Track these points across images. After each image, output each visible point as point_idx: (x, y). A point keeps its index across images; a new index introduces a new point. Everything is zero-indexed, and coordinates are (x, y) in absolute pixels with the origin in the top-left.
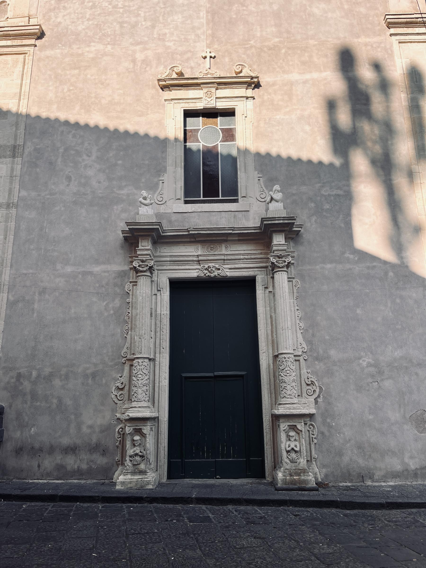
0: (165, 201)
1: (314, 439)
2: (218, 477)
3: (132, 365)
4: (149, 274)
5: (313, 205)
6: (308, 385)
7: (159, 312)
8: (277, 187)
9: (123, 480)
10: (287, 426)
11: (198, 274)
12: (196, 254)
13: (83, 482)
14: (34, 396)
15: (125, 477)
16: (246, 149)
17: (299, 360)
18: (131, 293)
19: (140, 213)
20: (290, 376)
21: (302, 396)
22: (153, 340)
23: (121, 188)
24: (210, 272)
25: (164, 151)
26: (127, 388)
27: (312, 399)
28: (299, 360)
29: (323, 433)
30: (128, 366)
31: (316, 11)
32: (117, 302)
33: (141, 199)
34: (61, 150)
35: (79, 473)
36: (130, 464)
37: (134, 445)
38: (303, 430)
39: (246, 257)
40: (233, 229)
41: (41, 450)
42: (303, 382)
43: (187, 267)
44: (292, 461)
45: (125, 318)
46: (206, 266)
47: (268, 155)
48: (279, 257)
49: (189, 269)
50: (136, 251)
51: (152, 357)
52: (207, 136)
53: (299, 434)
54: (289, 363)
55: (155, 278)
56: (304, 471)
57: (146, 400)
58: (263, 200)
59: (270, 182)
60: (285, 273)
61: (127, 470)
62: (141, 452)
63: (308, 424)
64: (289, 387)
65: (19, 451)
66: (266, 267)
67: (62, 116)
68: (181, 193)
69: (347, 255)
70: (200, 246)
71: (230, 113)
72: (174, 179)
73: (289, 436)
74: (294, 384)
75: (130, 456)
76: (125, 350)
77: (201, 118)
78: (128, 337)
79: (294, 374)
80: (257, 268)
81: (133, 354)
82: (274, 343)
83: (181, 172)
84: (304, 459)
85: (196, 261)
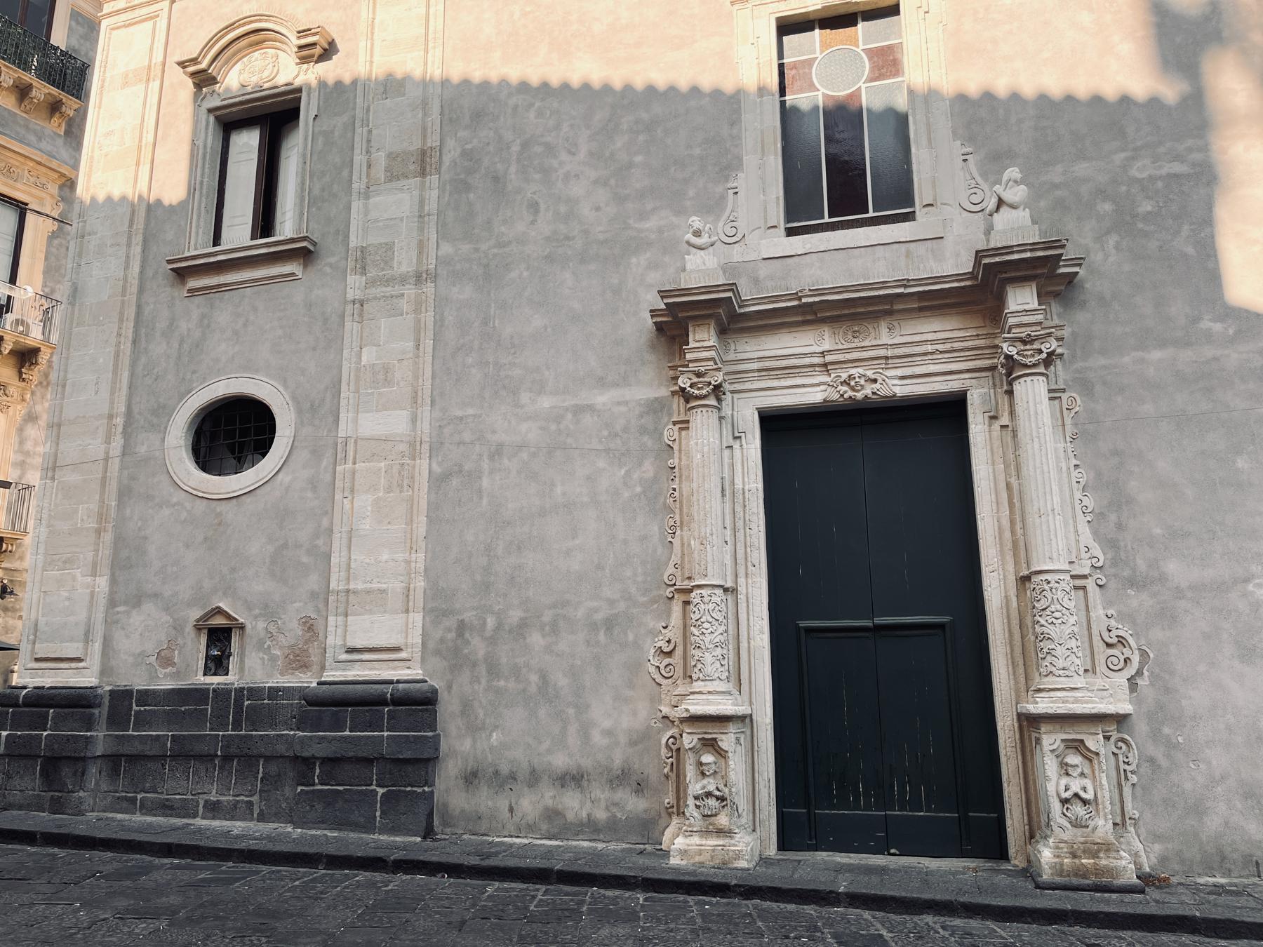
1: (1129, 775)
2: (893, 851)
3: (687, 603)
4: (713, 402)
5: (1107, 207)
6: (1109, 645)
7: (739, 484)
8: (1013, 172)
9: (685, 847)
10: (1058, 742)
11: (826, 394)
12: (821, 349)
13: (600, 846)
14: (493, 670)
15: (688, 841)
16: (930, 90)
17: (1084, 588)
18: (676, 447)
19: (689, 266)
20: (1063, 625)
21: (1094, 672)
22: (729, 548)
23: (643, 216)
24: (853, 389)
25: (735, 122)
26: (679, 652)
27: (1121, 679)
28: (1084, 588)
29: (1152, 760)
30: (680, 604)
32: (649, 469)
33: (689, 237)
34: (515, 148)
35: (590, 828)
36: (695, 814)
37: (703, 774)
38: (1102, 751)
39: (940, 347)
40: (906, 283)
41: (513, 777)
42: (1096, 639)
43: (799, 381)
44: (1076, 824)
45: (667, 502)
46: (844, 376)
47: (988, 96)
48: (1024, 342)
49: (804, 386)
50: (682, 354)
51: (729, 584)
52: (834, 71)
53: (1091, 761)
54: (1060, 594)
55: (726, 411)
57: (724, 677)
58: (977, 208)
59: (995, 162)
60: (1041, 378)
61: (690, 825)
62: (718, 789)
63: (1113, 739)
64: (1060, 651)
65: (471, 778)
66: (992, 368)
67: (514, 73)
68: (777, 212)
69: (1206, 324)
70: (826, 331)
72: (761, 182)
73: (1067, 764)
74: (1073, 643)
75: (696, 798)
76: (671, 570)
77: (817, 31)
78: (677, 542)
79: (1072, 620)
80: (968, 371)
81: (689, 578)
82: (1019, 547)
83: (775, 164)
84: (1106, 820)
85: (819, 365)
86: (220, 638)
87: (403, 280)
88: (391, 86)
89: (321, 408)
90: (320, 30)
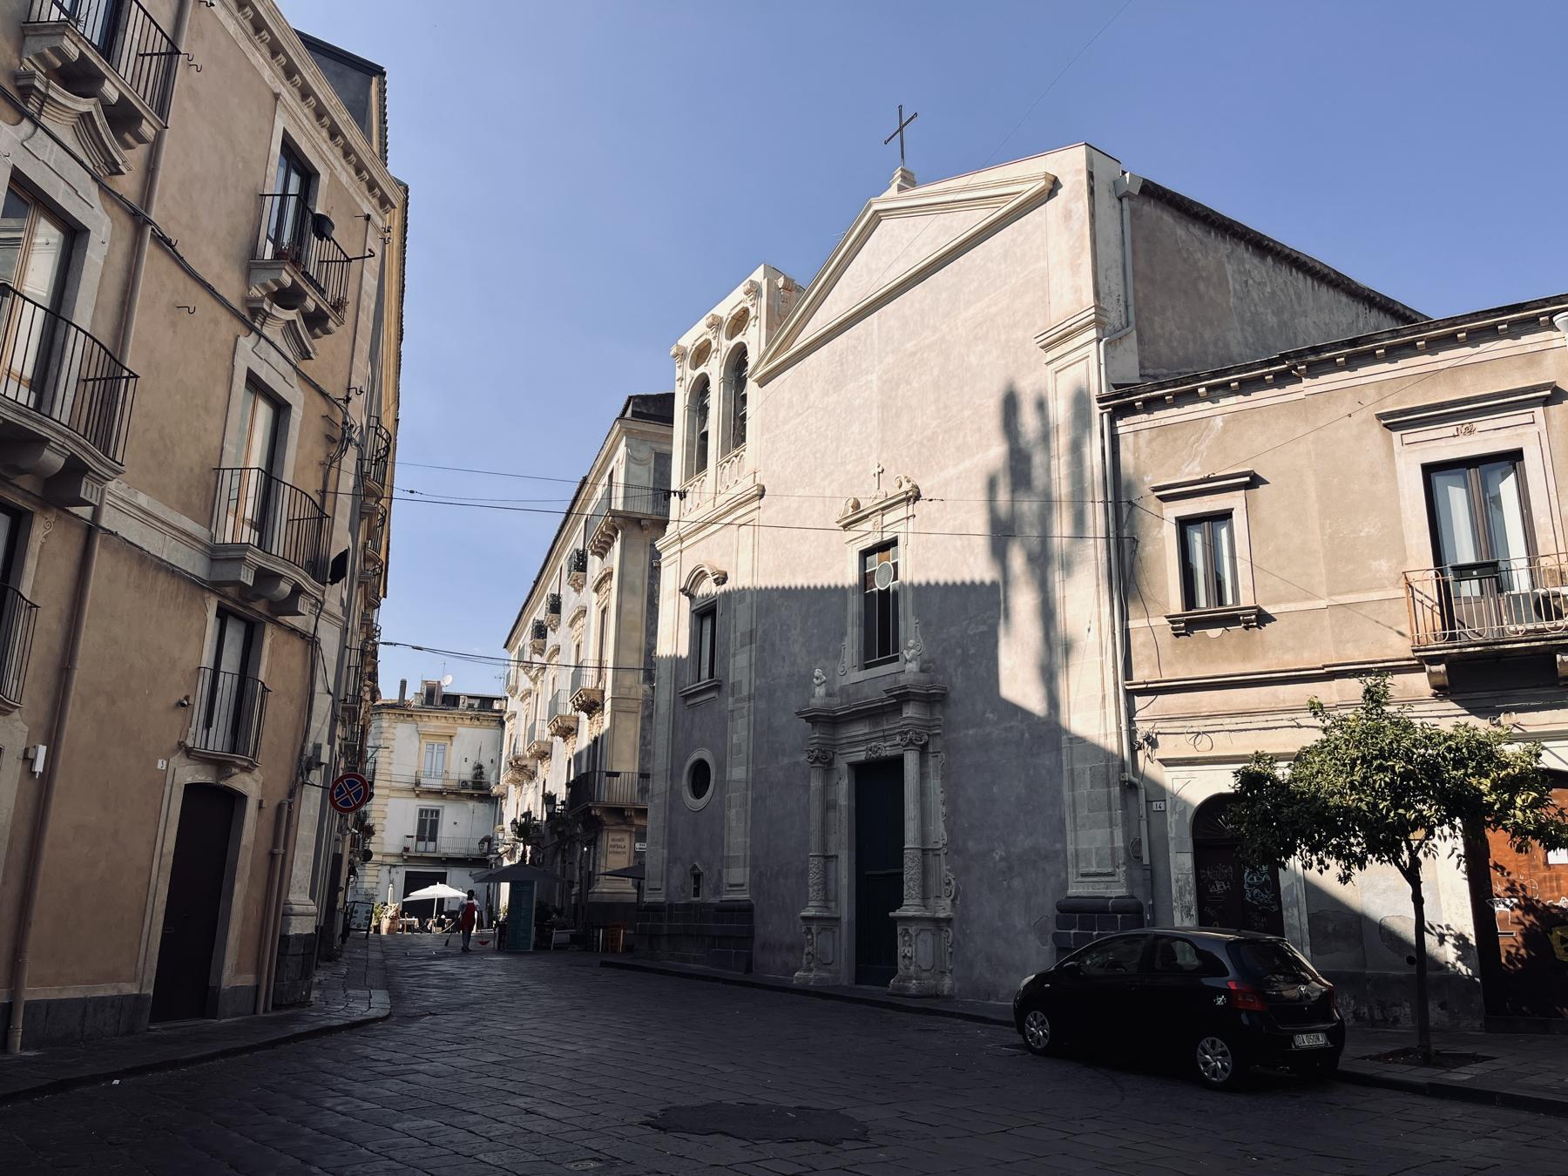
0: (846, 674)
31: (973, 360)
56: (910, 978)
71: (894, 543)
86: (697, 877)
87: (743, 700)
88: (742, 593)
89: (722, 767)
90: (719, 572)
